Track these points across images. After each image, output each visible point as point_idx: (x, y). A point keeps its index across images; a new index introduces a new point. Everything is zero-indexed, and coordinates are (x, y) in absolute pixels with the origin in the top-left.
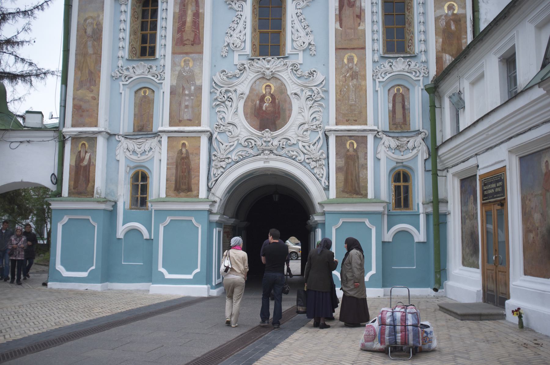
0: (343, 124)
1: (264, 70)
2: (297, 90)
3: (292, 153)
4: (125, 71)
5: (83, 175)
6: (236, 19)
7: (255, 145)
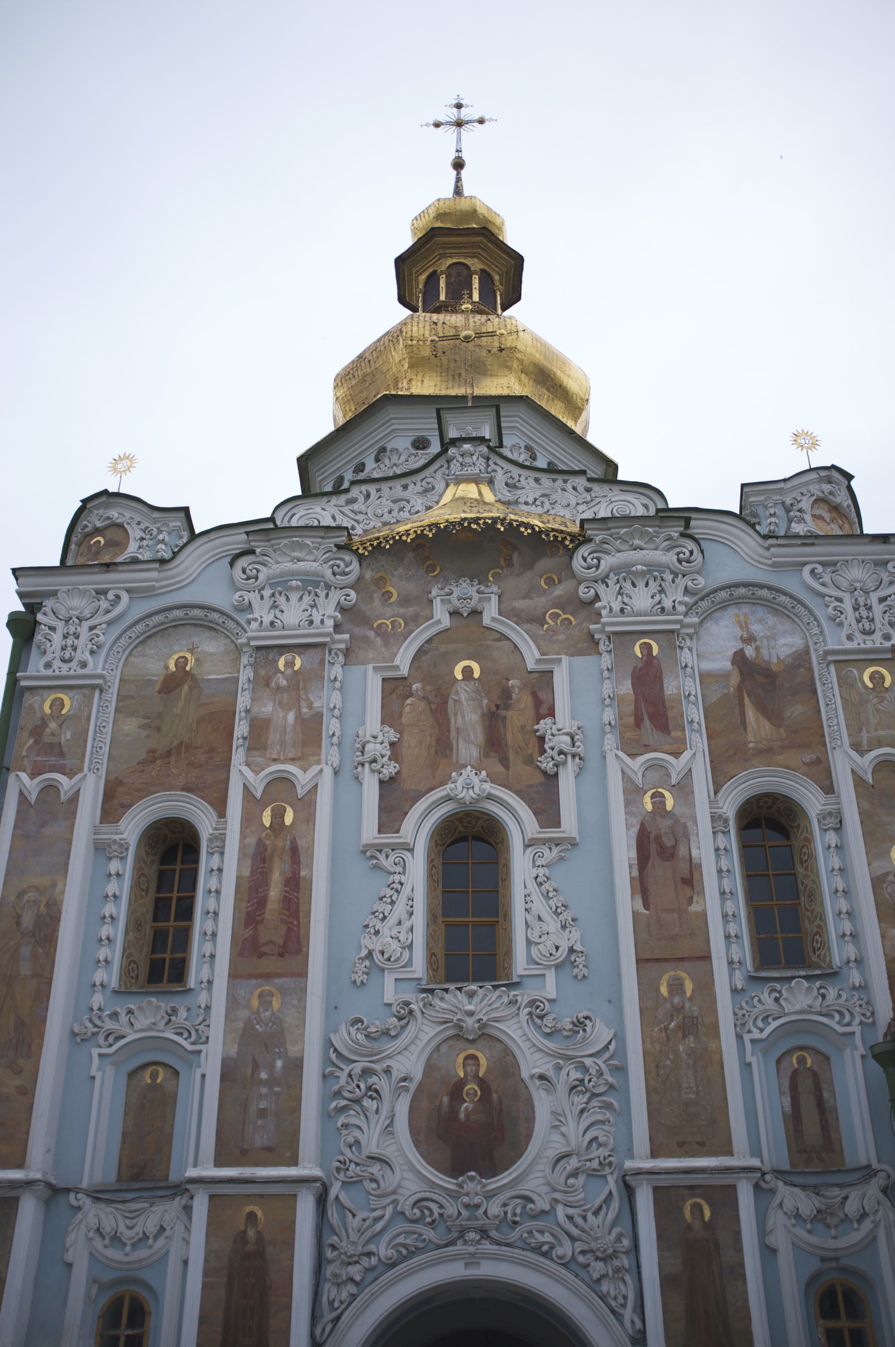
0: (670, 1155)
1: (459, 1016)
2: (545, 1066)
3: (541, 1239)
4: (107, 1020)
6: (389, 892)
7: (441, 1215)
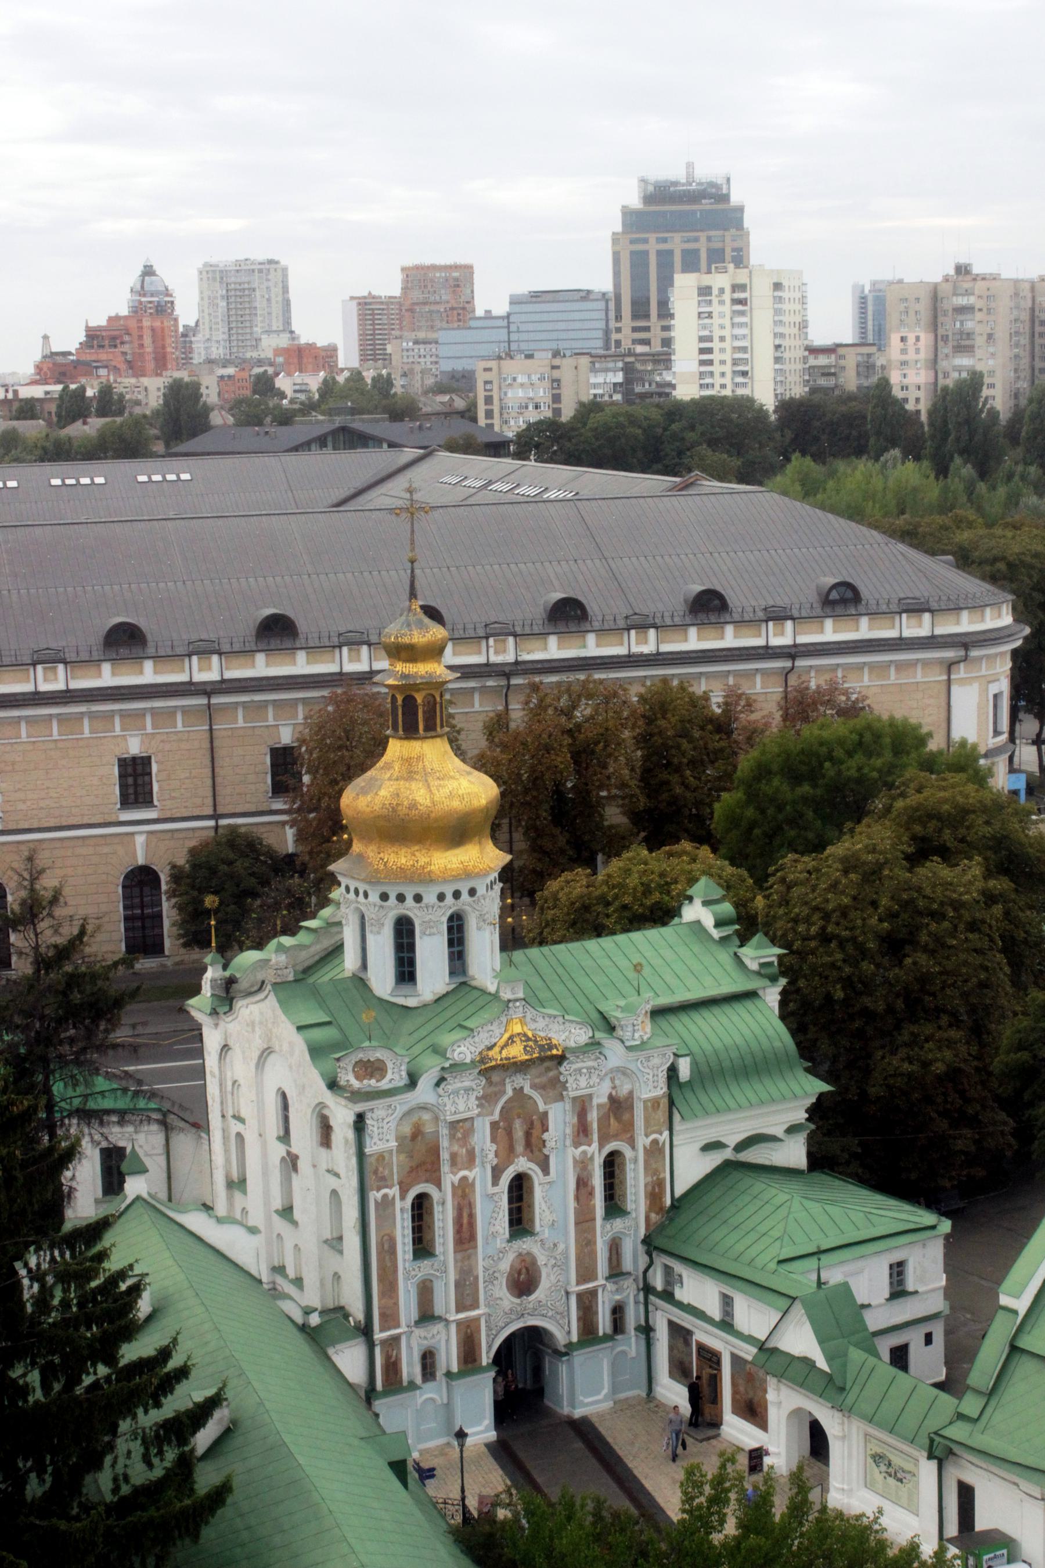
5: (392, 1367)
